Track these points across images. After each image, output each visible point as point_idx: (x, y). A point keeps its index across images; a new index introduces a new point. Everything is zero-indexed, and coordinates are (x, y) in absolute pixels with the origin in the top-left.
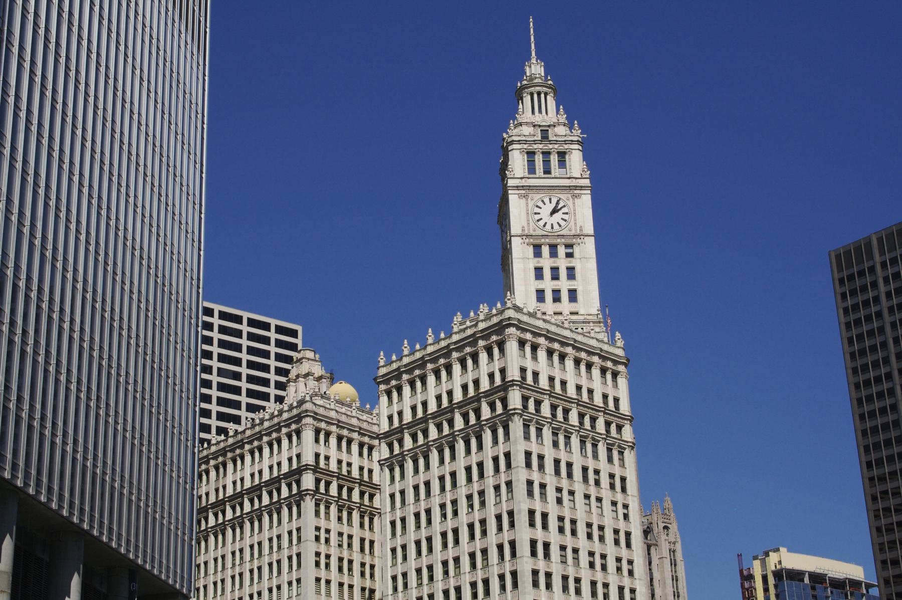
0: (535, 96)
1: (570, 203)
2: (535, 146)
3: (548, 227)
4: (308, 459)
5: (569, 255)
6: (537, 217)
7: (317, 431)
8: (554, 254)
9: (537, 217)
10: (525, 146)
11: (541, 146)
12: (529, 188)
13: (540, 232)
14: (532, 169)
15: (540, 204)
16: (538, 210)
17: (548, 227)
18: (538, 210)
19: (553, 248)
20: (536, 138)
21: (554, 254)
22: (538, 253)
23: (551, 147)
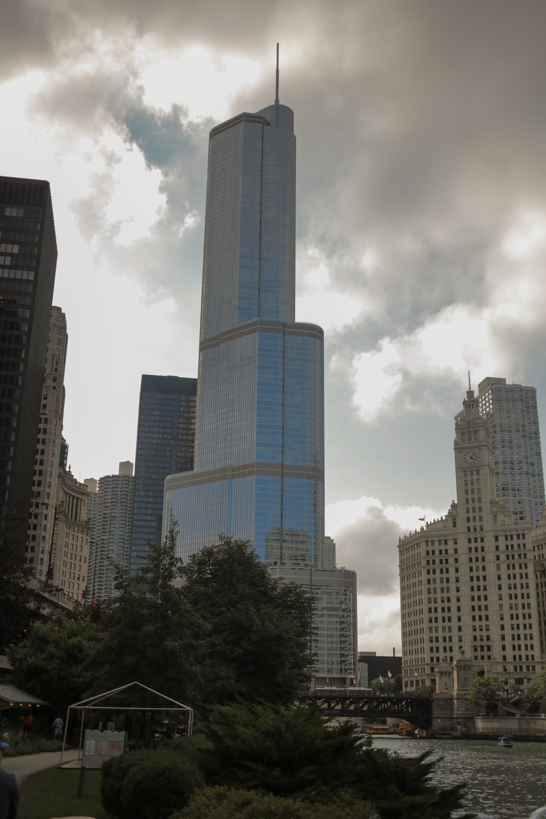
0: (468, 407)
2: (465, 430)
3: (469, 463)
5: (478, 473)
6: (465, 460)
8: (472, 474)
9: (465, 460)
10: (461, 430)
11: (467, 430)
12: (463, 449)
14: (464, 440)
15: (466, 454)
16: (465, 457)
17: (469, 463)
18: (465, 457)
19: (471, 471)
20: (466, 427)
21: (472, 474)
22: (466, 475)
23: (471, 429)
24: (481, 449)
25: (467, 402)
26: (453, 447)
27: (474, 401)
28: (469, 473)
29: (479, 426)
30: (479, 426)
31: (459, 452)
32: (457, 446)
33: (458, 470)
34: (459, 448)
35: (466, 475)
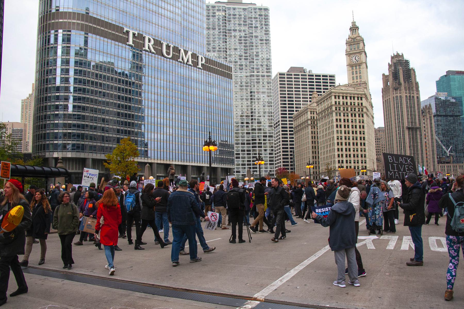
1: (359, 56)
4: (309, 118)
5: (360, 68)
7: (311, 112)
8: (356, 68)
13: (353, 64)
14: (351, 49)
21: (356, 68)
22: (352, 69)
24: (361, 54)
25: (352, 28)
26: (345, 53)
27: (356, 27)
28: (354, 68)
29: (360, 41)
30: (360, 41)
31: (348, 56)
32: (347, 53)
33: (348, 66)
34: (348, 54)
35: (352, 69)
